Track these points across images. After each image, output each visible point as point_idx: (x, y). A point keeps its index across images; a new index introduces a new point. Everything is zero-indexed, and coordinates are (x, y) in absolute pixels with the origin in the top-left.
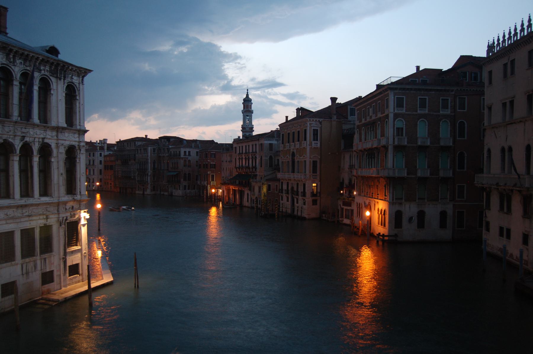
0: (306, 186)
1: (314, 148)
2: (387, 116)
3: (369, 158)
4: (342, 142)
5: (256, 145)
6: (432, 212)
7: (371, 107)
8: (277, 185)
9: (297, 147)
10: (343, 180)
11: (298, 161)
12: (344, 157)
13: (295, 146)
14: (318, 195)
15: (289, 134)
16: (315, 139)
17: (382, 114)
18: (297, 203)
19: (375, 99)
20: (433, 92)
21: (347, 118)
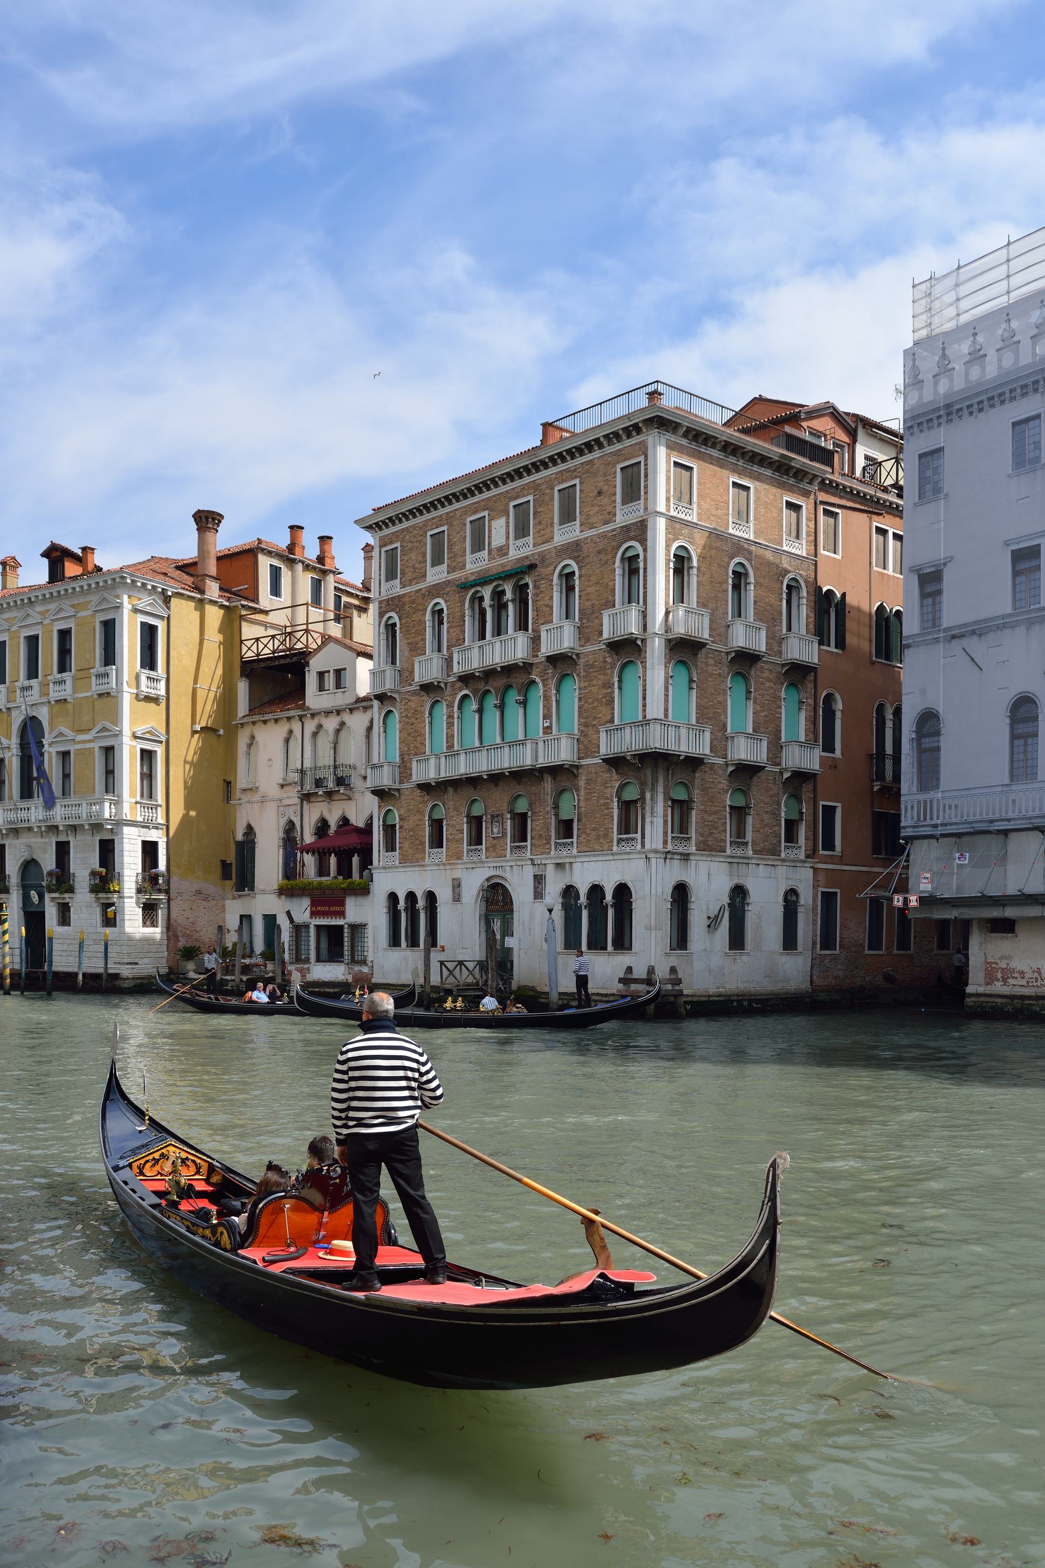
1: (148, 699)
3: (480, 711)
6: (766, 888)
10: (250, 830)
11: (65, 755)
16: (149, 660)
21: (256, 599)
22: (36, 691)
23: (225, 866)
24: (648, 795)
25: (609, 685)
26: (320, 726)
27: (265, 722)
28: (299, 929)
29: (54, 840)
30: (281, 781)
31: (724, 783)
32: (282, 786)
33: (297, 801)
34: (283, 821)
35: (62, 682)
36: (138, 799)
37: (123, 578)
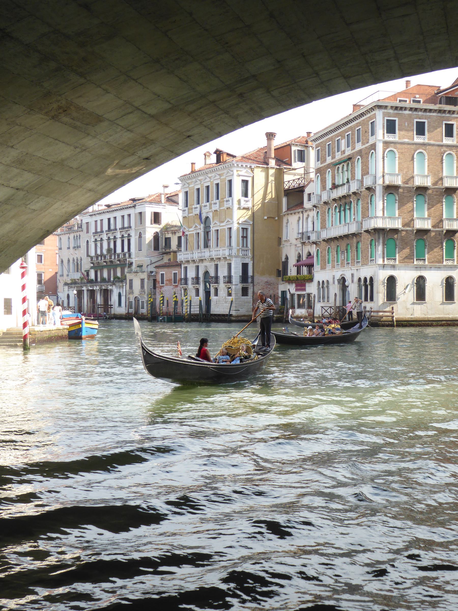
0: (233, 266)
2: (373, 147)
3: (340, 212)
4: (284, 200)
5: (129, 215)
7: (343, 137)
8: (175, 274)
9: (214, 209)
10: (287, 258)
12: (287, 223)
13: (210, 208)
14: (250, 280)
15: (198, 190)
16: (245, 194)
17: (363, 144)
18: (216, 294)
19: (349, 125)
20: (435, 114)
21: (291, 165)
22: (208, 207)
23: (279, 271)
24: (377, 244)
25: (368, 203)
26: (308, 215)
27: (291, 214)
28: (292, 295)
29: (226, 262)
30: (296, 238)
31: (413, 237)
32: (296, 239)
33: (301, 245)
34: (297, 253)
35: (216, 204)
36: (240, 247)
37: (233, 164)
